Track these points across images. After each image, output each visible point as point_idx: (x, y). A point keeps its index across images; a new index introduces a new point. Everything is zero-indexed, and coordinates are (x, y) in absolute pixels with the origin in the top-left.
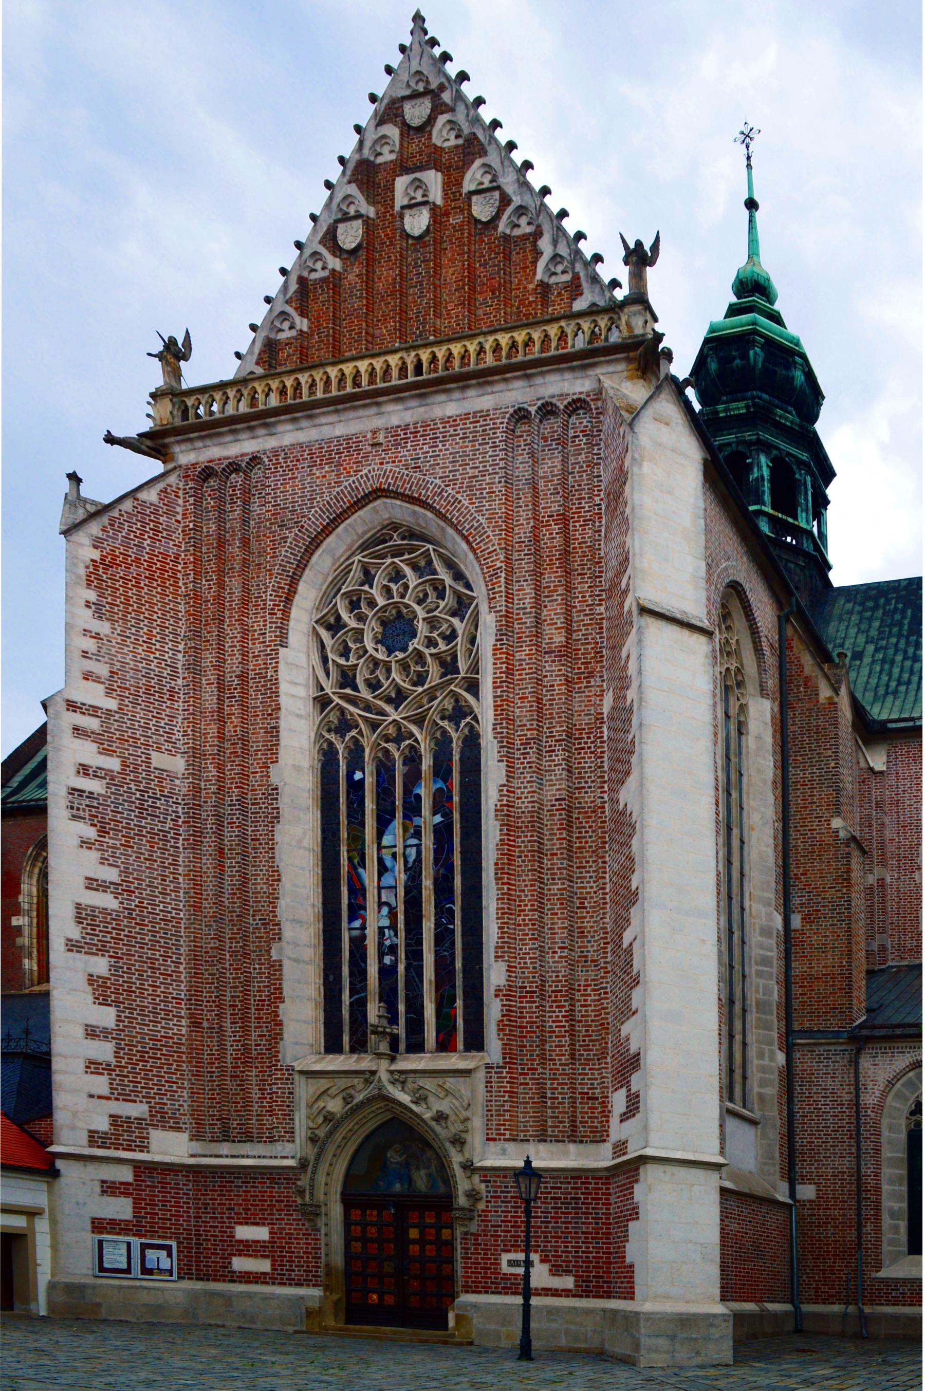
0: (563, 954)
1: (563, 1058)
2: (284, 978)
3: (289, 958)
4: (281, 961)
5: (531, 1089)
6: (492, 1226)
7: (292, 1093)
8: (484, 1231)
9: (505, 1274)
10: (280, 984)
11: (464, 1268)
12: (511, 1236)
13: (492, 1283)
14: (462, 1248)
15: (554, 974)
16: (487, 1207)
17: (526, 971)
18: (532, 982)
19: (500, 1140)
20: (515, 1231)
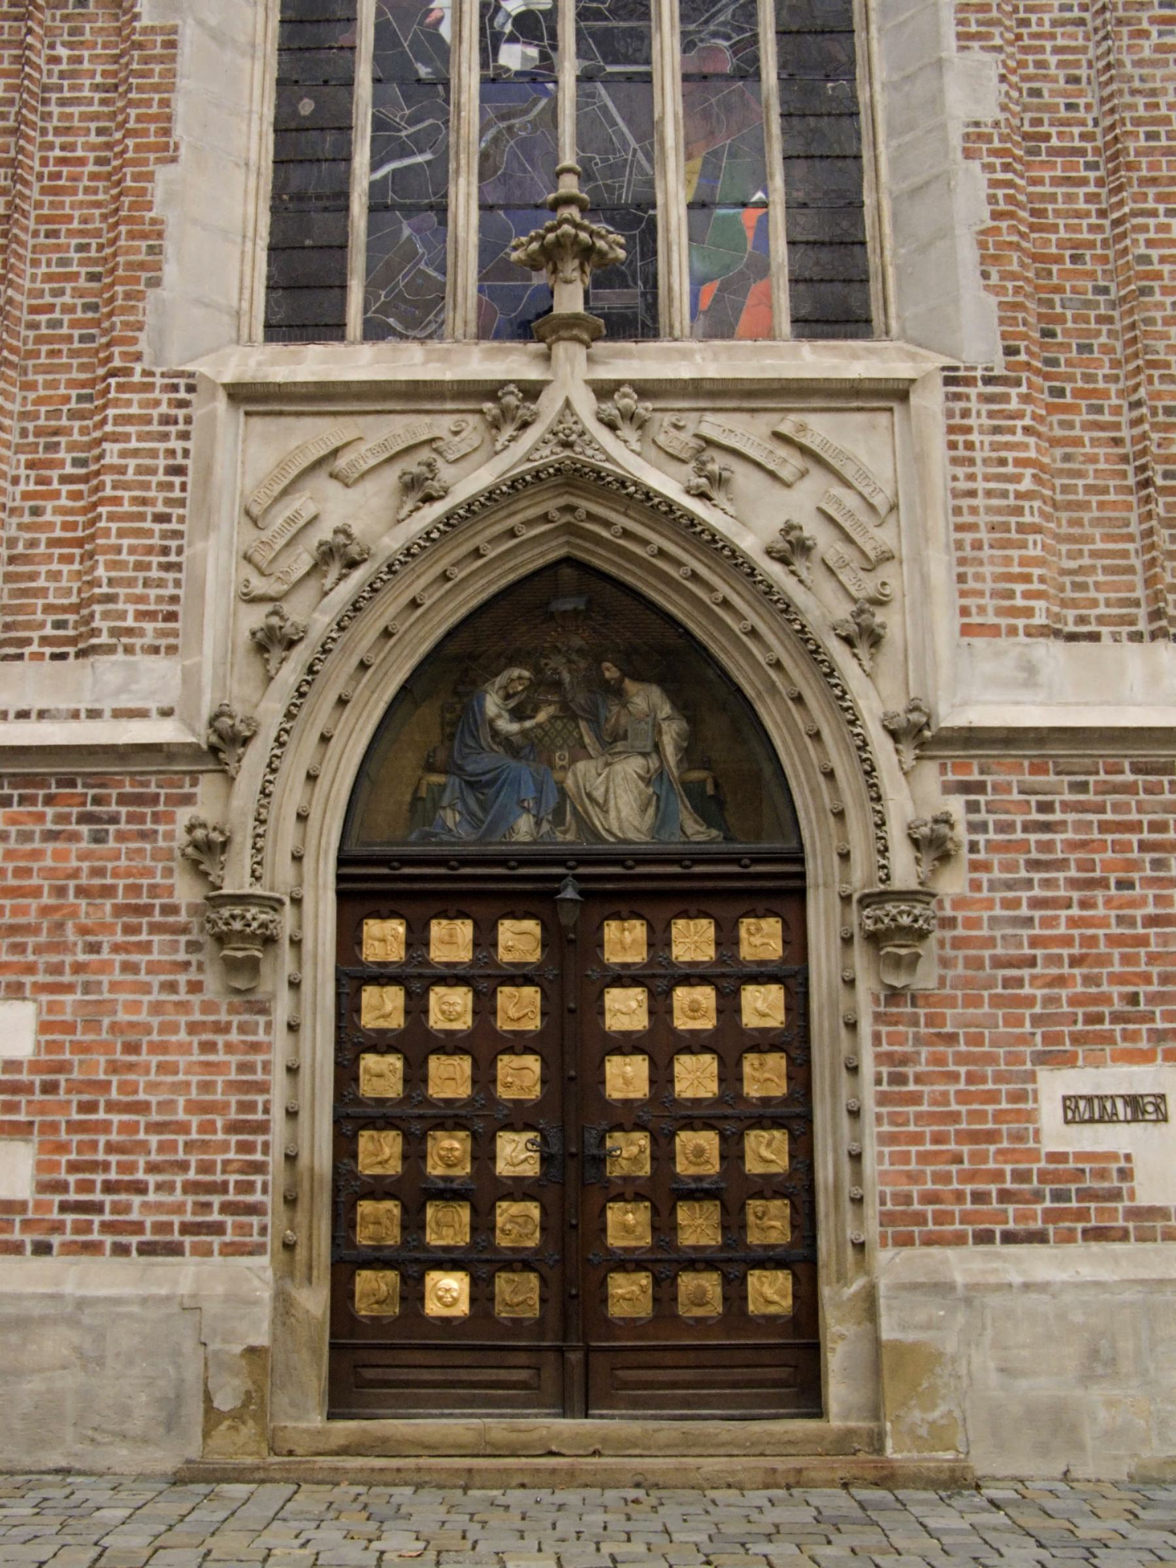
2: (182, 83)
3: (201, 23)
4: (174, 30)
5: (1093, 459)
6: (998, 963)
7: (180, 470)
8: (967, 983)
10: (165, 103)
11: (892, 1139)
12: (1074, 1001)
14: (880, 1058)
16: (976, 886)
17: (1045, 87)
19: (1012, 631)
20: (1088, 980)
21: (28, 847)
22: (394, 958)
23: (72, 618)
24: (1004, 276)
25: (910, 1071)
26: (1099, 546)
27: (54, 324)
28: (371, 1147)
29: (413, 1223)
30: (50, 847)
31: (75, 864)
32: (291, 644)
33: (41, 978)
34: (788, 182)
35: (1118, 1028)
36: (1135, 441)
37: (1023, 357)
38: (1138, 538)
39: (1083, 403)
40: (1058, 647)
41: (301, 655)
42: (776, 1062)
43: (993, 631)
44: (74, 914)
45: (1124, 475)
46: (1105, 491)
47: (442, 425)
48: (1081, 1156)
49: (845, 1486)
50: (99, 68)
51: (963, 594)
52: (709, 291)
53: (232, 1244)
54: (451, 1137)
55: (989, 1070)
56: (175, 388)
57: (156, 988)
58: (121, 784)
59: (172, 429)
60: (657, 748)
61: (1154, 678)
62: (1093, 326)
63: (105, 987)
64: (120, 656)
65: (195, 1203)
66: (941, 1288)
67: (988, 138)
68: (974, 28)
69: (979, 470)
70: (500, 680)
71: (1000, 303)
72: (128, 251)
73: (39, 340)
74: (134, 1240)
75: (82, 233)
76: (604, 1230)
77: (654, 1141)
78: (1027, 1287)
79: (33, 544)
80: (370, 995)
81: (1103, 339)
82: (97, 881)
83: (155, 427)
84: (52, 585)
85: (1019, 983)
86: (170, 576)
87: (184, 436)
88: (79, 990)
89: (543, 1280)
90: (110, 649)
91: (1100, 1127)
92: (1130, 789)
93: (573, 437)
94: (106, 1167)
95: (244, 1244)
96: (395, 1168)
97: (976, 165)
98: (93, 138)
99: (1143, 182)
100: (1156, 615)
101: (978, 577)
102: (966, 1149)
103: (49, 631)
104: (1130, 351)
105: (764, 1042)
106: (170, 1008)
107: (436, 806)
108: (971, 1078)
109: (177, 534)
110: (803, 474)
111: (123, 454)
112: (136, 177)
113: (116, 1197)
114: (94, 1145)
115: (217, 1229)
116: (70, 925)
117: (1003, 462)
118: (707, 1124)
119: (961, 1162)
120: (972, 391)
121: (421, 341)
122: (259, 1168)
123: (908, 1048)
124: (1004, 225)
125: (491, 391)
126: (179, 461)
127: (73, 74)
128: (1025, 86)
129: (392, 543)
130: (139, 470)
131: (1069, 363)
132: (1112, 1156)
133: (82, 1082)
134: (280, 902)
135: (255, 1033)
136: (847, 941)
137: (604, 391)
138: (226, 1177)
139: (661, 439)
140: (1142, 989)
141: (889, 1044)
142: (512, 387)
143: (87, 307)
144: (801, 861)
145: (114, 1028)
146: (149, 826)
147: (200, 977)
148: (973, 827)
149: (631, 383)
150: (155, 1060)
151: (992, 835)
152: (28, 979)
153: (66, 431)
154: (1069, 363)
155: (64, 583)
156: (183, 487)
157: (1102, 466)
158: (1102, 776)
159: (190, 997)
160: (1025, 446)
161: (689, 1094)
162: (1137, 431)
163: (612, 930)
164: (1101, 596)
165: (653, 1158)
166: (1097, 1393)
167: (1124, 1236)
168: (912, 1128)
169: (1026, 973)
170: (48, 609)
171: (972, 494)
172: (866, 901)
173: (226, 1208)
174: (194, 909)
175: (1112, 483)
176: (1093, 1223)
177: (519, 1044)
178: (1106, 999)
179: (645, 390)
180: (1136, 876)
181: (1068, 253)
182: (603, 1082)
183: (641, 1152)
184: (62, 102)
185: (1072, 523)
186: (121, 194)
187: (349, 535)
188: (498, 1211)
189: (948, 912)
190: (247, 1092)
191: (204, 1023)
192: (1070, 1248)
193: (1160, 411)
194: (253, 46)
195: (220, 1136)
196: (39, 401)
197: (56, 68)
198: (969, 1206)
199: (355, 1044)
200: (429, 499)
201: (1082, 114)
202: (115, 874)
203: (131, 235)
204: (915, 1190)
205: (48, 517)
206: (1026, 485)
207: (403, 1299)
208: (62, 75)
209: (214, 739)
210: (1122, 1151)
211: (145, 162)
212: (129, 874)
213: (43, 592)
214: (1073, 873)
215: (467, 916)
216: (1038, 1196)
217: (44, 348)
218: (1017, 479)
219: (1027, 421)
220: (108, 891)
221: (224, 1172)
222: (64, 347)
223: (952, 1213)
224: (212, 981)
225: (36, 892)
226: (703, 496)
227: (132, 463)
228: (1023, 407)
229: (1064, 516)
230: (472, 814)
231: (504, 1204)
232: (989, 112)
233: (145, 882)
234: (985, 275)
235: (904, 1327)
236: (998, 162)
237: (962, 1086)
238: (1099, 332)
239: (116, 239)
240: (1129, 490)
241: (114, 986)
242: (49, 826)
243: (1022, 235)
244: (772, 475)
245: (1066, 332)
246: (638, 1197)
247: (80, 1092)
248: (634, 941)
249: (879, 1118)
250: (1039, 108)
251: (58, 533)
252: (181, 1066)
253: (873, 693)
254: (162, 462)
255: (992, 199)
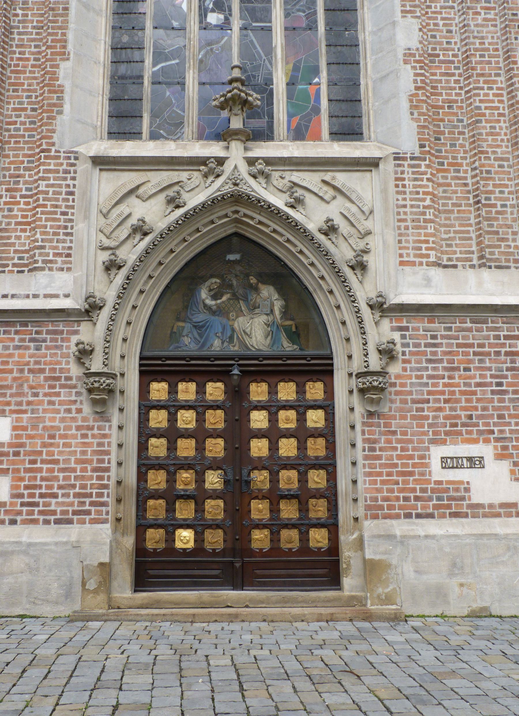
0: (488, 16)
1: (499, 150)
5: (456, 192)
6: (414, 401)
7: (72, 193)
8: (401, 410)
9: (440, 482)
10: (64, 34)
11: (370, 474)
12: (446, 418)
13: (417, 498)
14: (365, 441)
15: (477, 41)
16: (405, 369)
17: (438, 34)
18: (447, 50)
19: (421, 264)
20: (452, 409)
21: (7, 352)
22: (163, 398)
23: (26, 255)
24: (420, 114)
25: (377, 446)
26: (458, 228)
27: (16, 129)
28: (153, 477)
29: (171, 509)
30: (17, 352)
31: (28, 359)
32: (120, 267)
33: (13, 407)
34: (328, 75)
35: (464, 429)
36: (473, 184)
37: (427, 149)
38: (474, 225)
39: (452, 168)
40: (440, 271)
41: (123, 272)
42: (321, 442)
43: (413, 264)
44: (27, 380)
45: (468, 199)
46: (460, 205)
47: (184, 176)
48: (449, 482)
49: (351, 620)
50: (35, 19)
51: (400, 248)
52: (296, 120)
53: (94, 519)
54: (187, 473)
55: (410, 446)
56: (69, 158)
57: (62, 412)
58: (47, 326)
59: (69, 176)
60: (272, 311)
61: (480, 284)
62: (457, 136)
63: (41, 411)
64: (47, 272)
65: (79, 502)
66: (390, 537)
67: (414, 55)
68: (408, 8)
69: (408, 196)
70: (207, 284)
71: (418, 126)
72: (49, 98)
73: (11, 136)
74: (52, 518)
75: (29, 90)
76: (250, 511)
77: (271, 474)
78: (426, 537)
79: (9, 224)
80: (153, 413)
81: (461, 141)
82: (37, 367)
83: (61, 175)
84: (17, 242)
85: (423, 410)
86: (68, 238)
87: (74, 179)
88: (29, 412)
89: (225, 533)
90: (42, 269)
91: (457, 470)
92: (470, 330)
93: (238, 181)
94: (40, 487)
95: (99, 519)
96: (163, 486)
97: (409, 67)
98: (33, 49)
99: (479, 75)
100: (481, 257)
101: (407, 241)
102: (400, 479)
103: (16, 261)
104: (472, 146)
105: (316, 434)
106: (68, 420)
107: (181, 335)
108: (403, 449)
109: (71, 221)
110: (334, 198)
111: (47, 186)
112: (52, 66)
113: (45, 500)
114: (35, 478)
115: (88, 513)
116: (25, 385)
117: (418, 193)
118: (292, 467)
119: (399, 484)
120: (406, 163)
121: (175, 141)
122: (106, 487)
123: (376, 437)
124: (420, 92)
125: (203, 161)
126: (72, 189)
127: (24, 21)
128: (429, 34)
129: (161, 225)
130: (54, 193)
131: (446, 151)
132: (462, 482)
133: (30, 451)
134: (116, 375)
135: (105, 430)
136: (351, 392)
137: (251, 162)
138: (91, 491)
139: (275, 183)
140: (474, 413)
141: (369, 435)
142: (212, 160)
143: (31, 123)
144: (332, 359)
145: (44, 428)
146: (59, 343)
147: (81, 407)
148: (404, 345)
149: (263, 158)
150: (62, 441)
151: (411, 349)
152: (7, 408)
153: (23, 176)
154: (446, 151)
155: (23, 241)
156: (73, 201)
157: (459, 195)
158: (458, 324)
159: (76, 415)
160: (427, 186)
161: (285, 455)
162: (475, 180)
163: (253, 387)
164: (458, 250)
165: (270, 481)
166: (455, 581)
167: (466, 516)
168: (378, 470)
169: (425, 406)
170: (15, 252)
171: (405, 206)
172: (359, 375)
173: (92, 504)
174: (79, 378)
175: (463, 202)
176: (453, 510)
177: (215, 434)
178: (459, 417)
179: (269, 161)
180: (472, 366)
181: (446, 105)
182: (249, 450)
183: (265, 478)
184: (19, 34)
185: (446, 219)
186: (45, 73)
187: (144, 222)
188: (206, 503)
189: (393, 380)
190: (101, 455)
191: (83, 426)
192: (444, 521)
193: (484, 172)
194: (101, 10)
195: (90, 473)
196: (11, 163)
197: (17, 19)
198: (402, 503)
199: (147, 434)
200: (178, 207)
201: (453, 46)
202: (45, 363)
203: (50, 92)
204: (379, 495)
205: (15, 212)
206: (428, 202)
207: (166, 541)
208: (19, 22)
209: (87, 306)
210: (465, 480)
211: (55, 60)
212: (51, 363)
213: (13, 244)
214: (445, 365)
215: (194, 381)
216: (430, 499)
217: (13, 140)
218: (424, 200)
219: (429, 176)
220: (42, 371)
221: (91, 488)
222: (21, 140)
223: (395, 505)
224: (87, 409)
225: (11, 371)
226: (292, 207)
227: (51, 190)
228: (427, 170)
229: (443, 216)
230: (195, 338)
231: (209, 501)
232: (414, 44)
233: (58, 367)
234: (412, 114)
235: (375, 553)
236: (418, 65)
237: (399, 452)
238: (459, 139)
239: (44, 93)
240: (470, 205)
241: (45, 411)
242: (17, 343)
243: (427, 96)
244: (321, 198)
245: (445, 138)
246: (264, 498)
247: (29, 456)
248: (262, 392)
249: (364, 465)
250: (435, 43)
251: (20, 220)
252: (73, 444)
253: (362, 289)
254: (64, 190)
255: (415, 81)
